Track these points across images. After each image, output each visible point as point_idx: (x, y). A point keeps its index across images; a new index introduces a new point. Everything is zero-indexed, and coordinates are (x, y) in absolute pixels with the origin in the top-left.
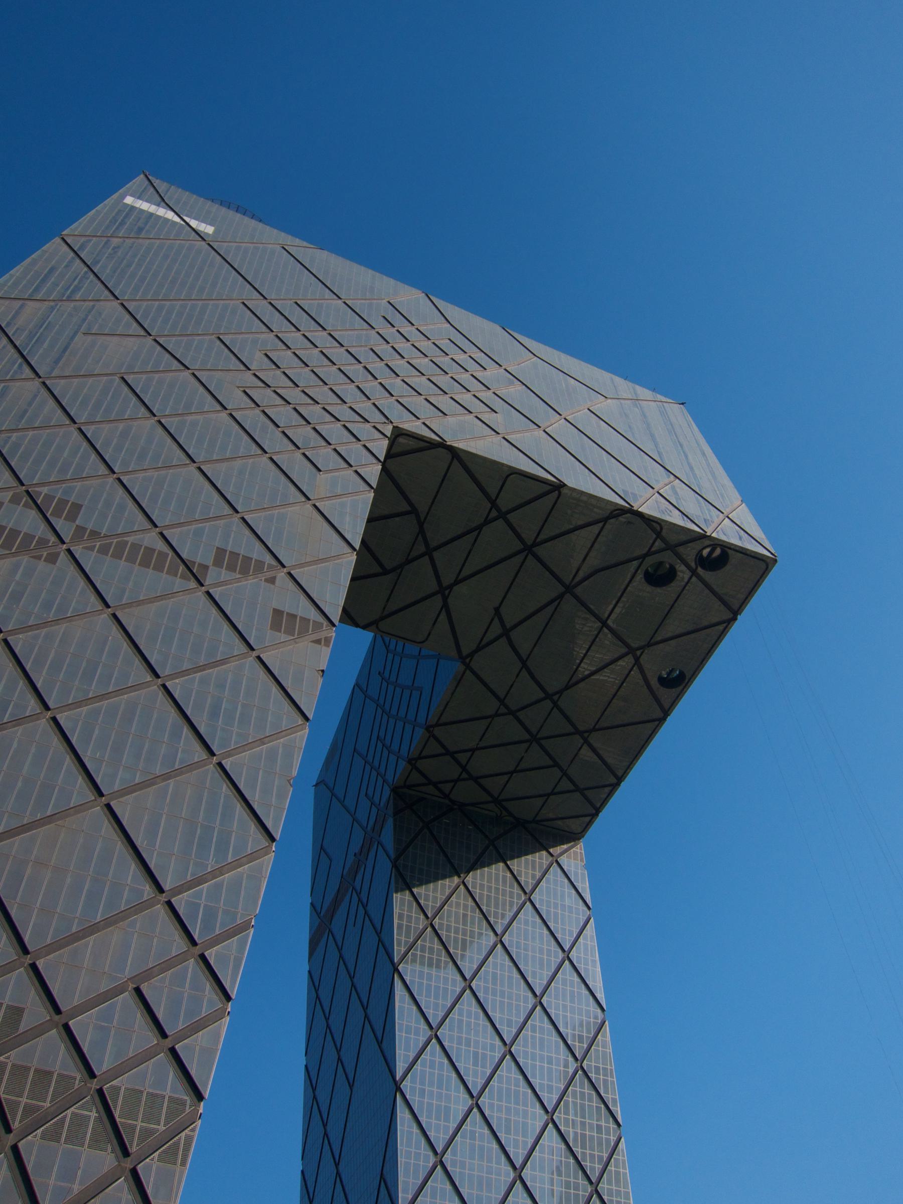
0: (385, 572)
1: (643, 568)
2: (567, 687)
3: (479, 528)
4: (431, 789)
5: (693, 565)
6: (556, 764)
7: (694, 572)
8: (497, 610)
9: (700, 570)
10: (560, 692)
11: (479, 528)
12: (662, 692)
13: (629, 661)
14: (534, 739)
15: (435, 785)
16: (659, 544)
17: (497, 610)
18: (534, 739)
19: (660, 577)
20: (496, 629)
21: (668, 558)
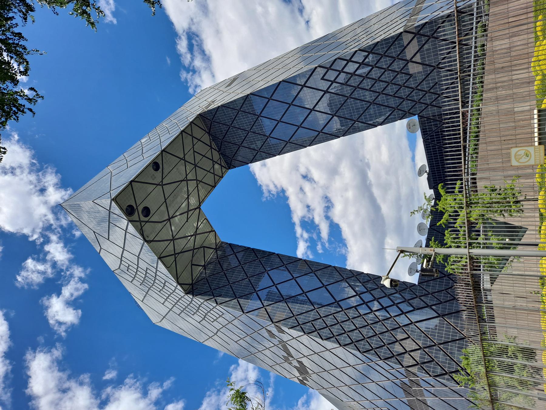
0: (204, 247)
1: (149, 217)
2: (182, 181)
3: (181, 252)
4: (223, 164)
5: (136, 212)
6: (194, 151)
7: (137, 208)
8: (187, 221)
9: (135, 208)
10: (184, 180)
11: (181, 252)
12: (160, 162)
13: (165, 182)
14: (196, 166)
15: (220, 165)
16: (143, 224)
17: (187, 221)
18: (196, 166)
19: (147, 211)
20: (190, 213)
21: (143, 218)
